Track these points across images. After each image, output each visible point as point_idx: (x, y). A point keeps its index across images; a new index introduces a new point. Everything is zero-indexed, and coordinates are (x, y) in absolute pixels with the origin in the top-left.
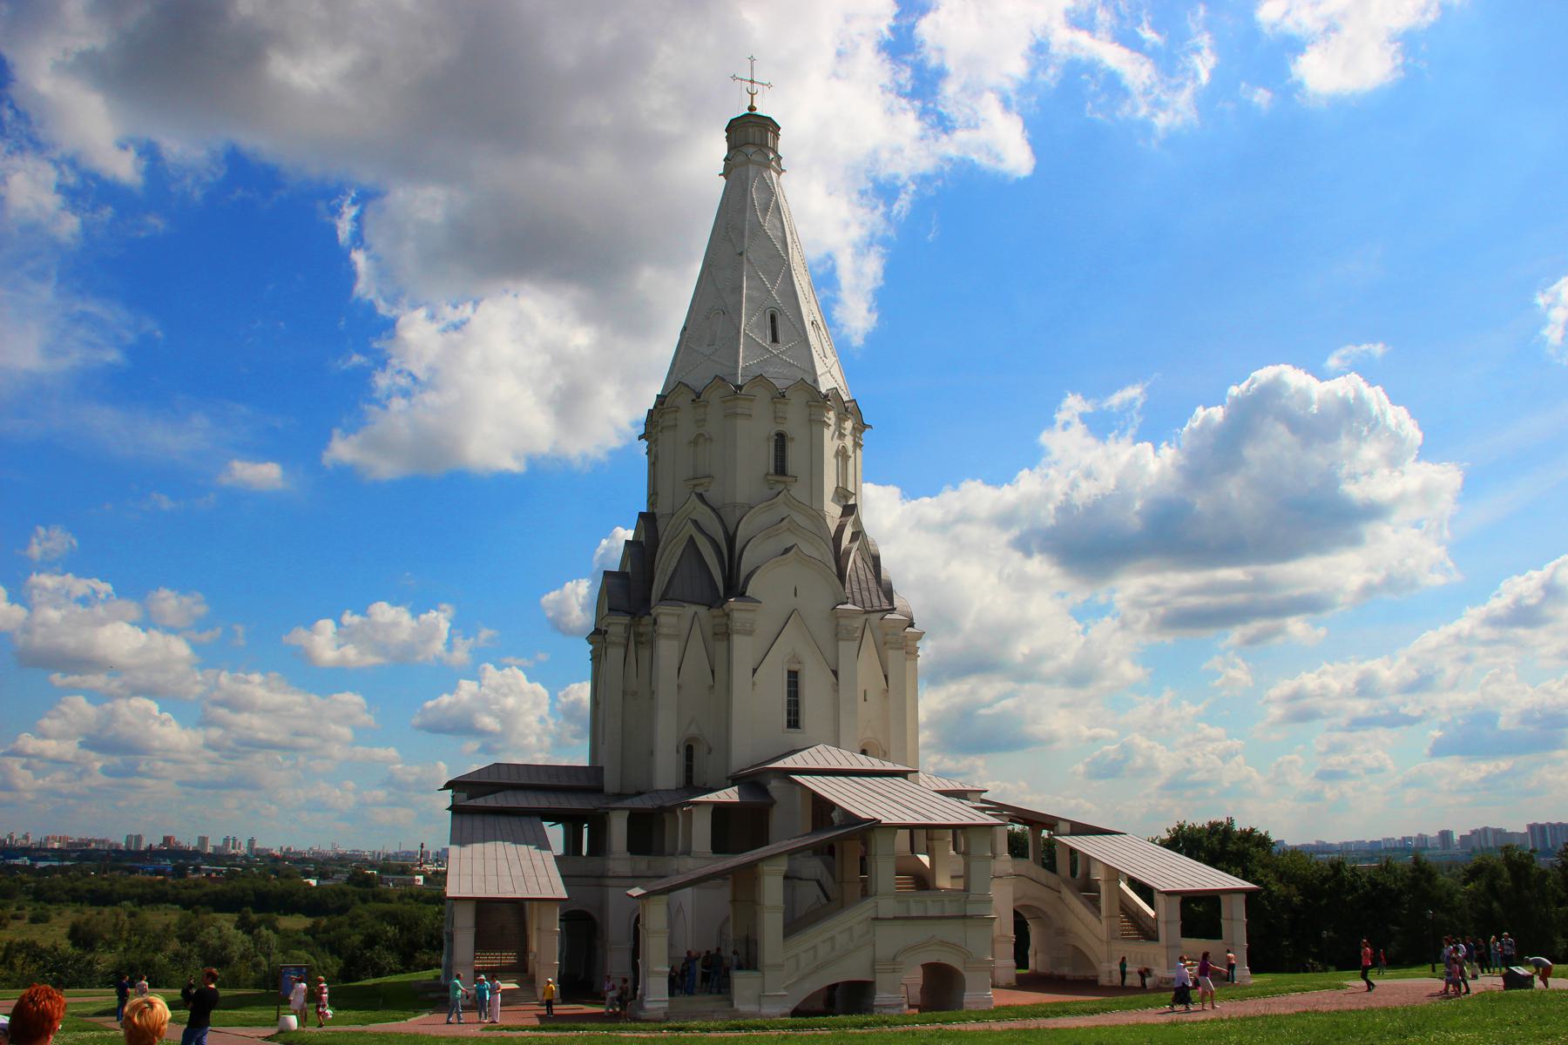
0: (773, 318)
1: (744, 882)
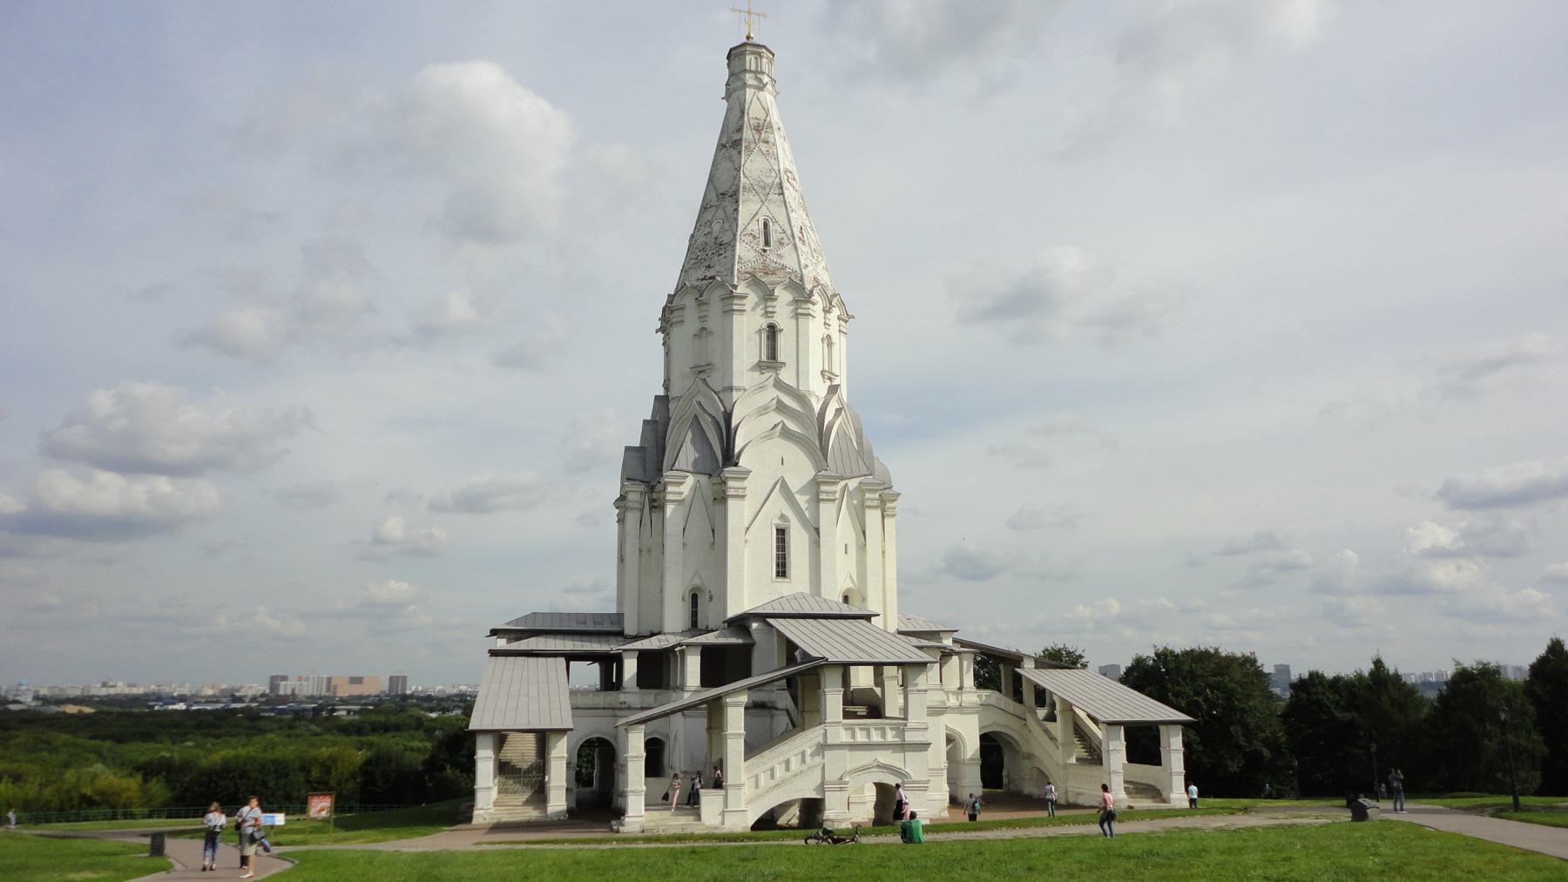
1: (715, 709)
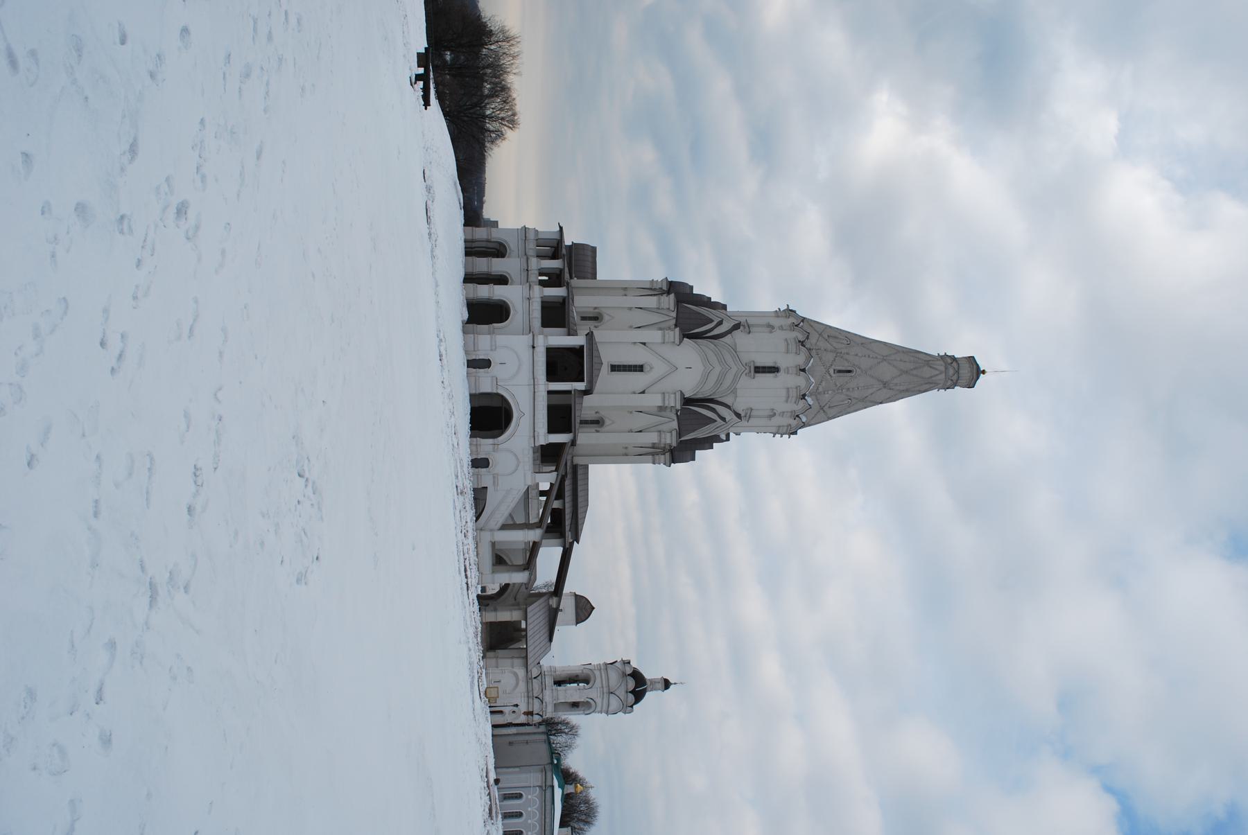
0: (850, 371)
